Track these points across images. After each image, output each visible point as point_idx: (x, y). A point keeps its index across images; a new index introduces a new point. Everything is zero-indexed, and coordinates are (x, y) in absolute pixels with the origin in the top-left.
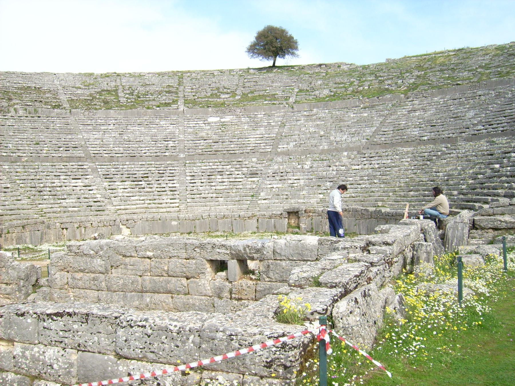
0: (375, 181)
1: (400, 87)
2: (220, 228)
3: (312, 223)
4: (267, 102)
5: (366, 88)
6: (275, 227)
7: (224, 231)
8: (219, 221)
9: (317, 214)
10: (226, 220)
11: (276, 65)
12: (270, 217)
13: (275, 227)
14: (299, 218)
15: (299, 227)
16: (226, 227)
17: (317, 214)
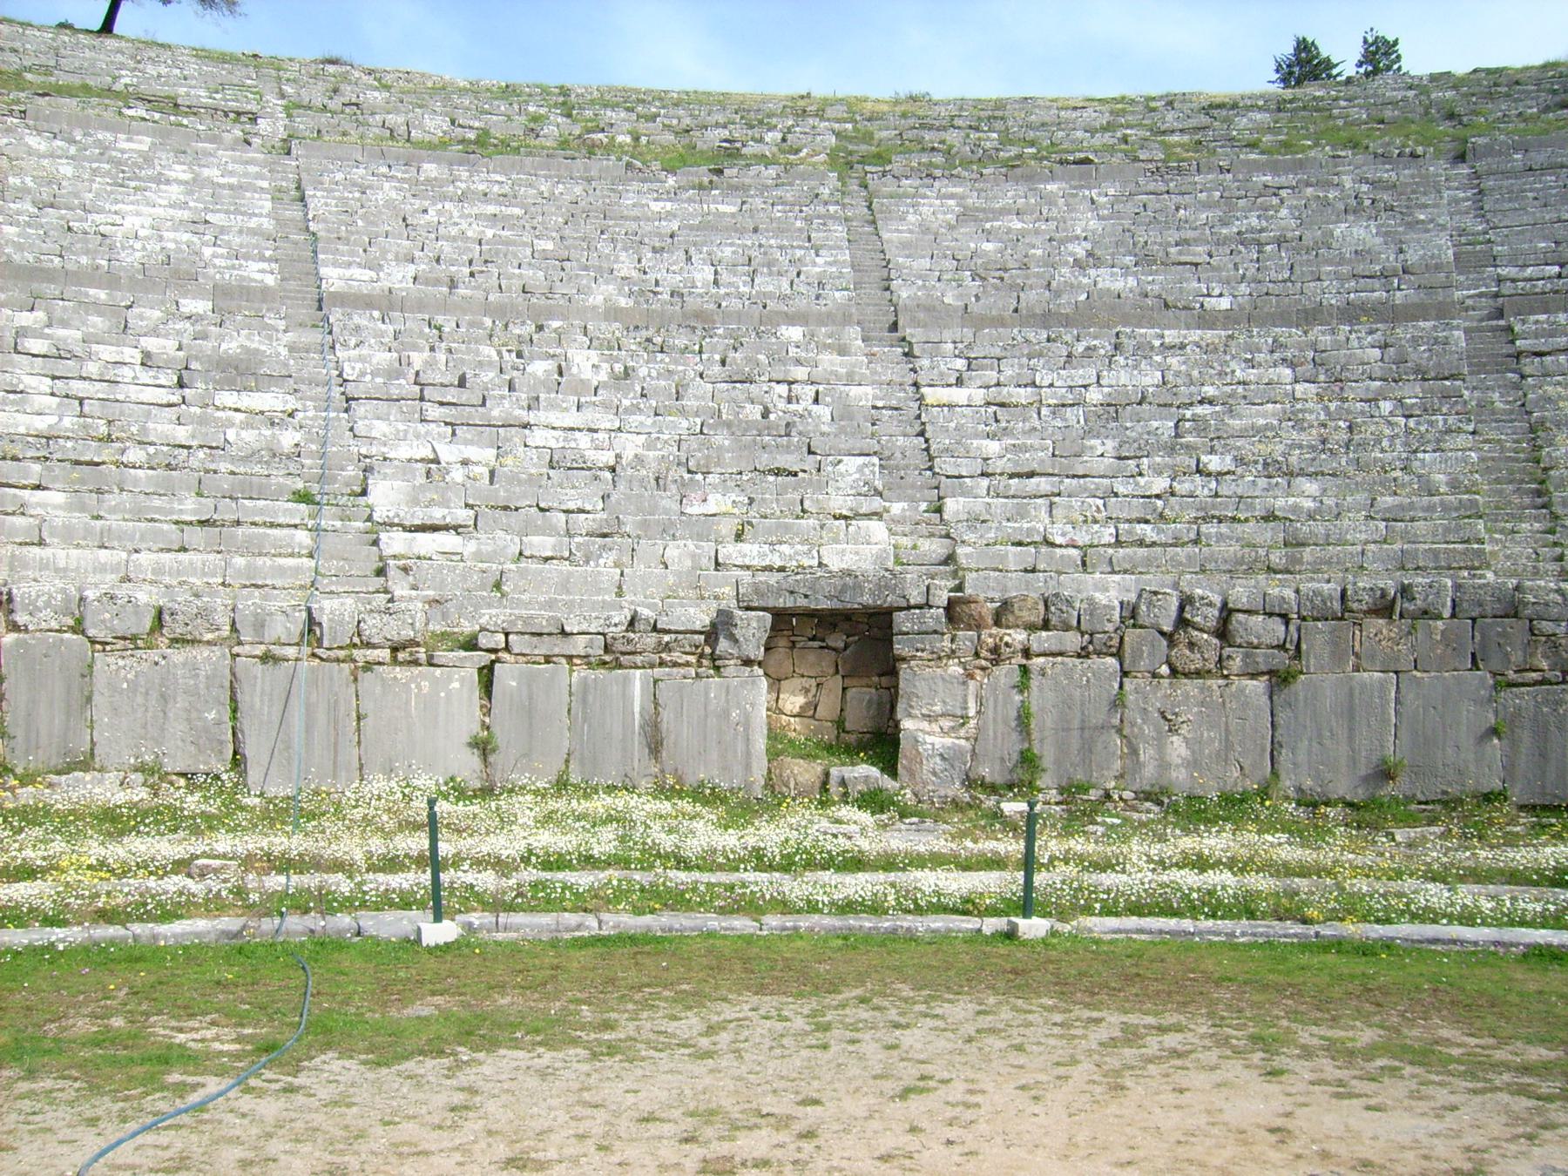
0: (1214, 463)
1: (797, 151)
2: (113, 733)
3: (1023, 720)
4: (142, 113)
5: (620, 139)
6: (655, 747)
7: (153, 773)
8: (107, 664)
9: (1073, 640)
10: (178, 656)
11: (116, 30)
12: (613, 655)
13: (655, 747)
14: (889, 668)
15: (883, 744)
16: (177, 728)
17: (1073, 640)
